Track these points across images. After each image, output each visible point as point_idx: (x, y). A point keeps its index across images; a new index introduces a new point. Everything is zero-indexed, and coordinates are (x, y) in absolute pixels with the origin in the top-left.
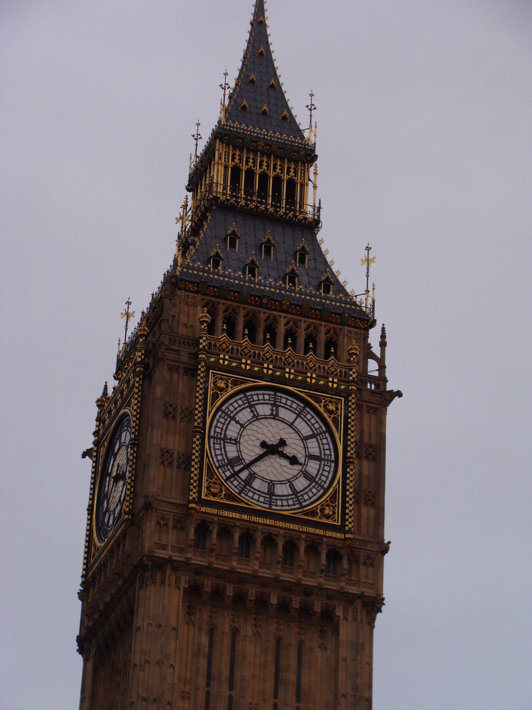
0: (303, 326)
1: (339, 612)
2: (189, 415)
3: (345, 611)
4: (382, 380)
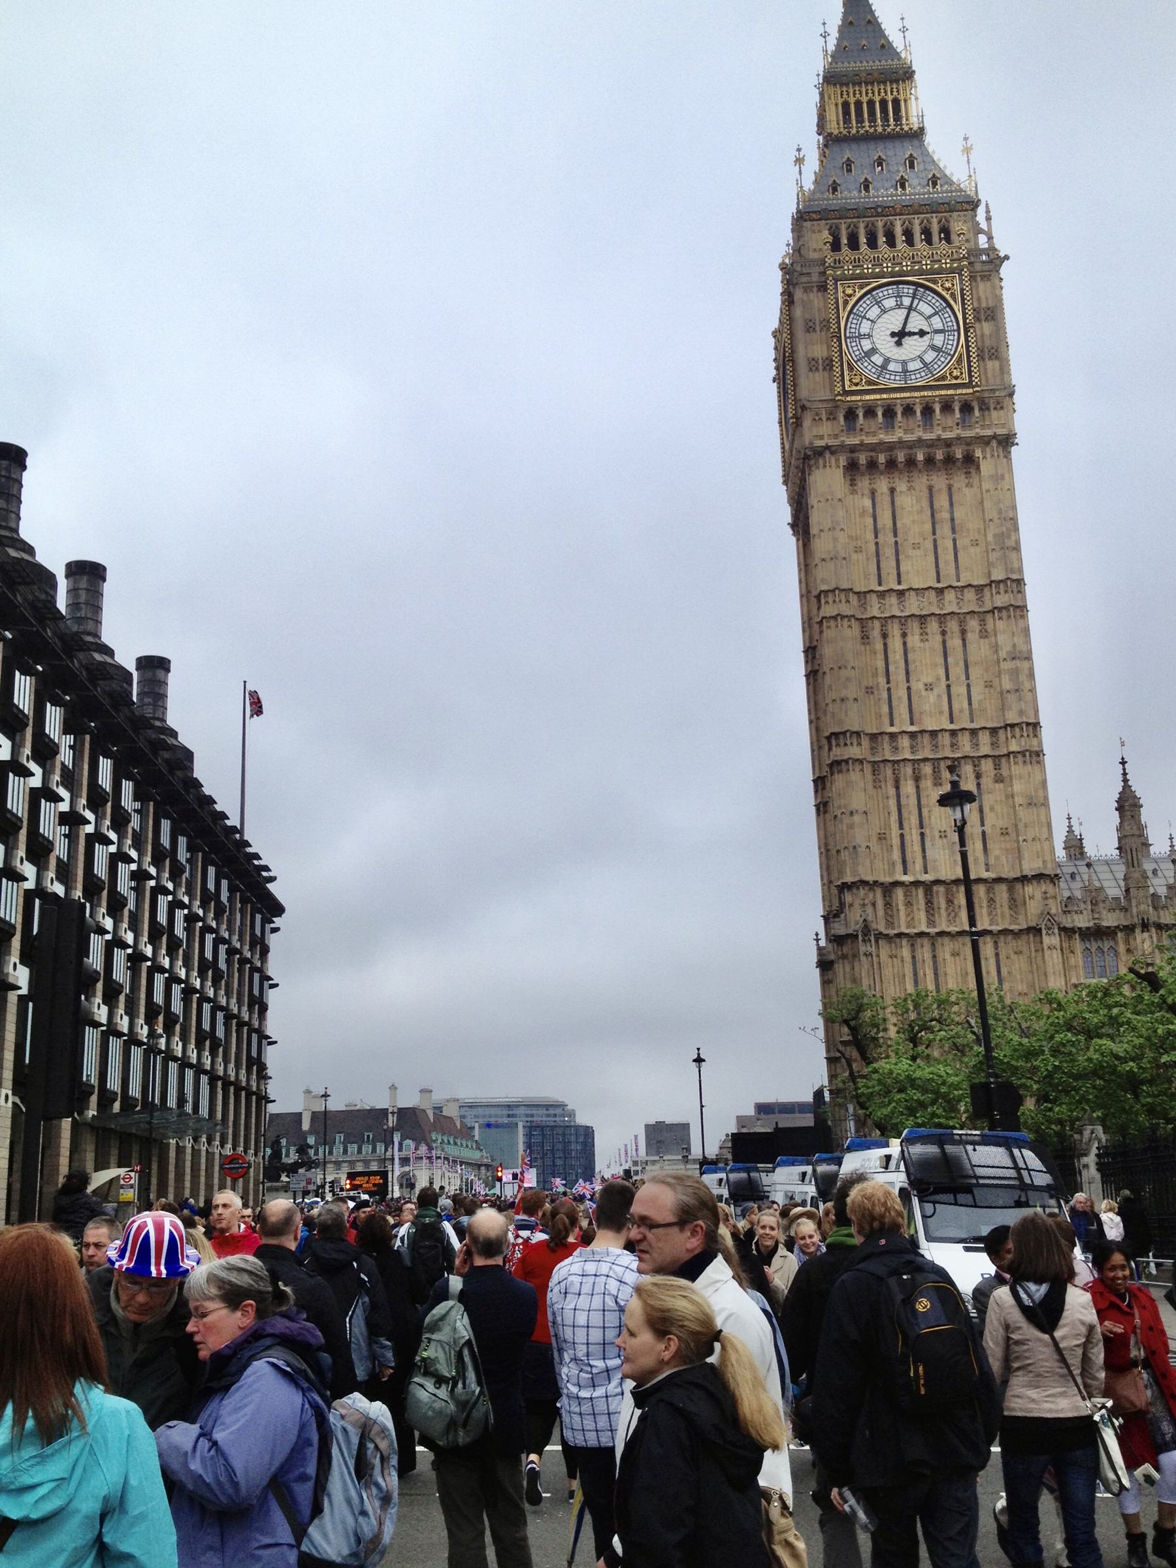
0: (917, 222)
1: (978, 453)
2: (826, 324)
4: (992, 249)
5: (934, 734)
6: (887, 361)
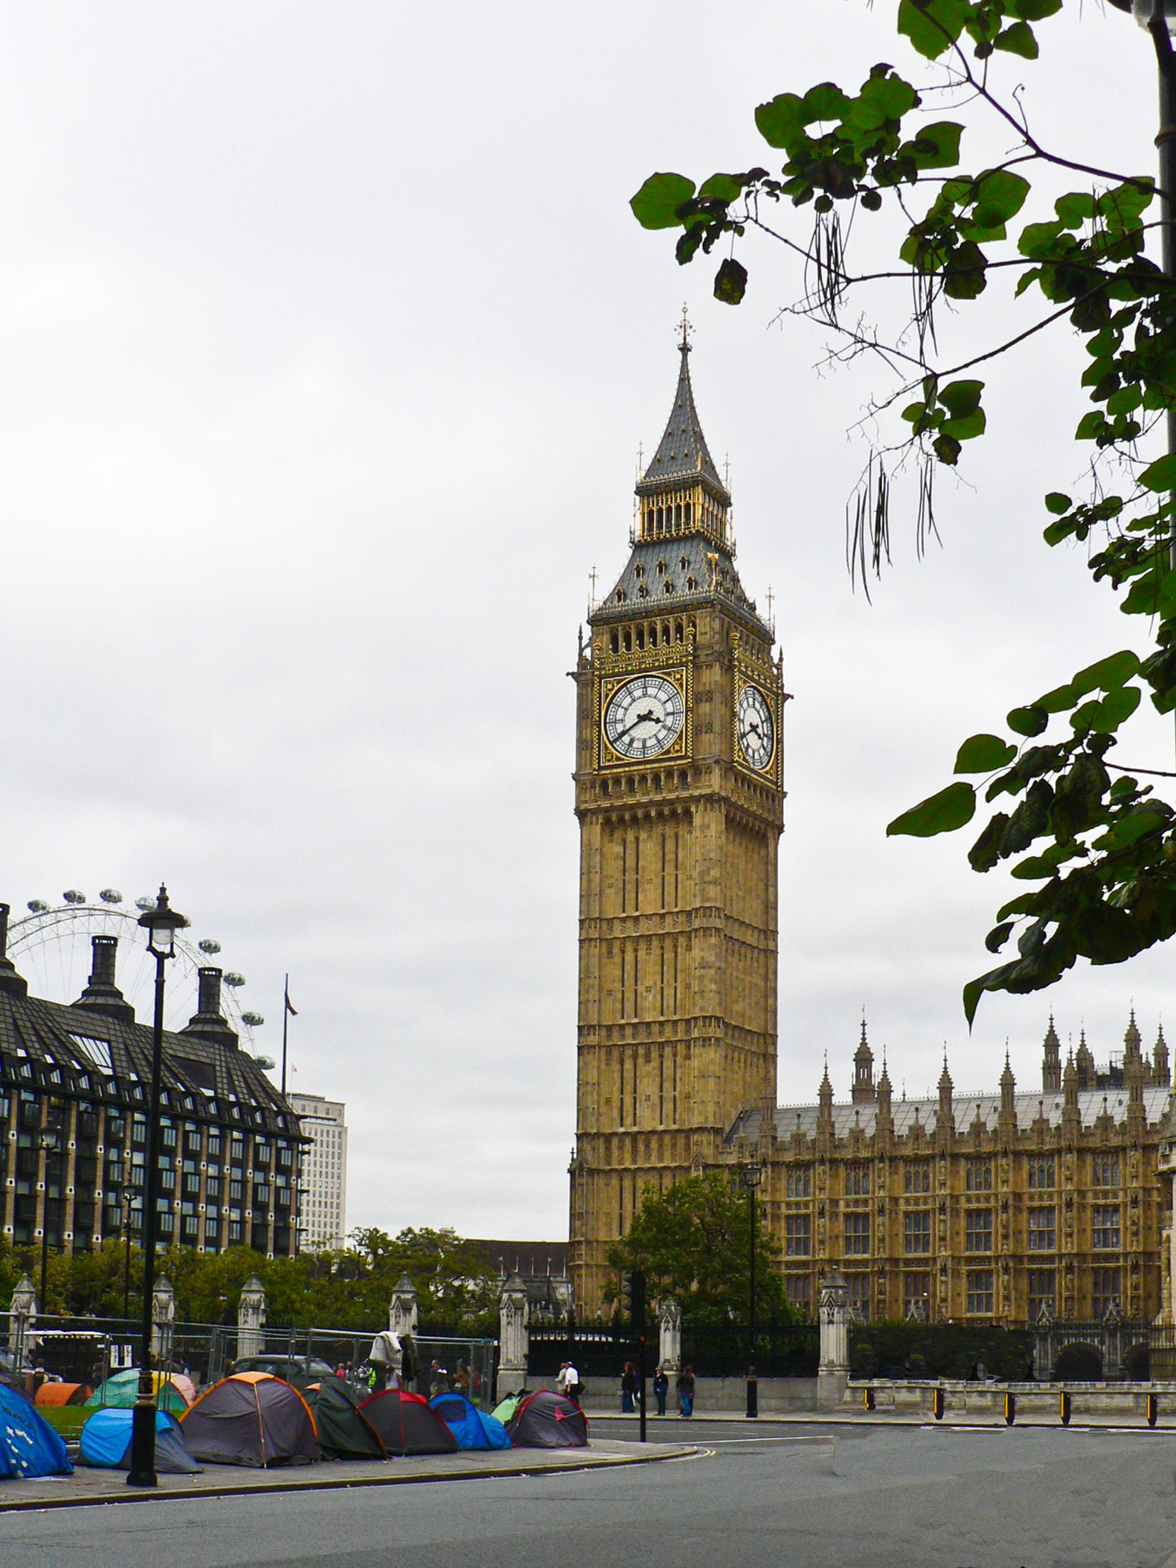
1: (693, 809)
3: (697, 807)
5: (648, 1024)
6: (632, 741)
